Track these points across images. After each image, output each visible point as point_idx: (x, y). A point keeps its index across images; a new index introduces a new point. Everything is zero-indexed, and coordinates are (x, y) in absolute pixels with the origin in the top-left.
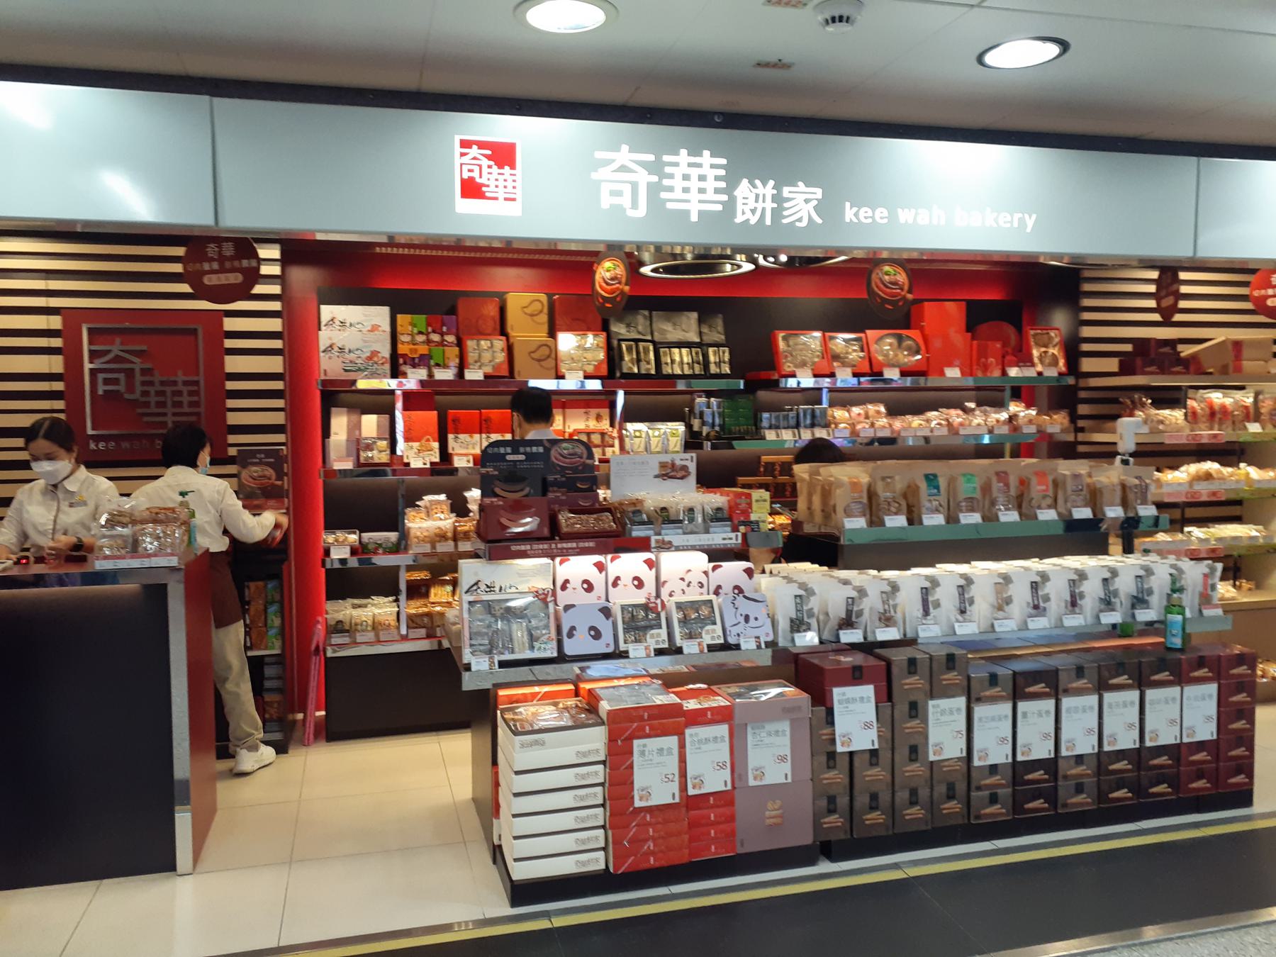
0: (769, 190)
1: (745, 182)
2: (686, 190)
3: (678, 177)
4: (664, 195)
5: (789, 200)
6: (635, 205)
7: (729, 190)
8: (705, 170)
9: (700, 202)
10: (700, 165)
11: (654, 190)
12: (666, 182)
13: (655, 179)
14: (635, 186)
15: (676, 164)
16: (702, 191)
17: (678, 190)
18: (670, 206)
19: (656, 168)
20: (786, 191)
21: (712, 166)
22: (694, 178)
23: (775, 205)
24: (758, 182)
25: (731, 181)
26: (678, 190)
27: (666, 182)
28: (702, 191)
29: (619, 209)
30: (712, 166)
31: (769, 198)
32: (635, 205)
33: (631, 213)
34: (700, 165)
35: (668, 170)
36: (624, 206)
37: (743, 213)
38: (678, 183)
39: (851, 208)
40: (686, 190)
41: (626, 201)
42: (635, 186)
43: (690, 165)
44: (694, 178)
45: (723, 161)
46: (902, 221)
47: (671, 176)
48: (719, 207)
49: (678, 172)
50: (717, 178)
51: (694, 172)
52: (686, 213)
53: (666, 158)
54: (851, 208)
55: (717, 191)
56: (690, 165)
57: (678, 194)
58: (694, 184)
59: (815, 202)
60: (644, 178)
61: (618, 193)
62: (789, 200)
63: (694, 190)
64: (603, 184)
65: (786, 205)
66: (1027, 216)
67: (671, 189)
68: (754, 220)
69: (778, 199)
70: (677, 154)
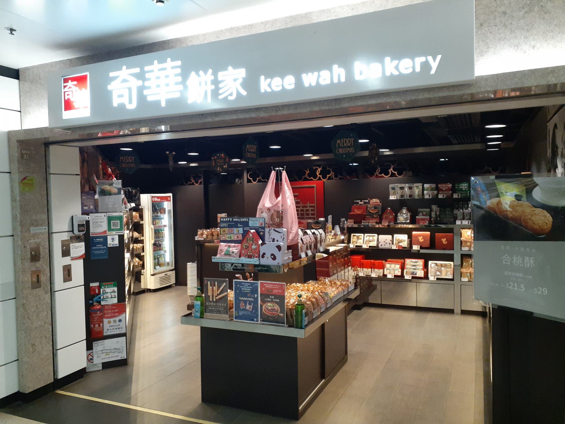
0: (209, 76)
1: (193, 74)
2: (158, 86)
5: (222, 81)
6: (130, 102)
7: (184, 82)
11: (141, 90)
13: (140, 83)
14: (130, 89)
15: (152, 71)
16: (167, 85)
18: (149, 99)
19: (141, 76)
20: (221, 75)
23: (213, 87)
24: (201, 72)
25: (185, 75)
28: (167, 85)
30: (173, 68)
31: (209, 83)
36: (125, 103)
39: (265, 80)
40: (158, 86)
45: (179, 63)
46: (306, 84)
47: (149, 79)
50: (176, 75)
54: (265, 80)
55: (177, 84)
59: (241, 80)
60: (135, 83)
61: (120, 96)
62: (222, 81)
65: (220, 86)
66: (430, 58)
69: (216, 82)
70: (152, 64)
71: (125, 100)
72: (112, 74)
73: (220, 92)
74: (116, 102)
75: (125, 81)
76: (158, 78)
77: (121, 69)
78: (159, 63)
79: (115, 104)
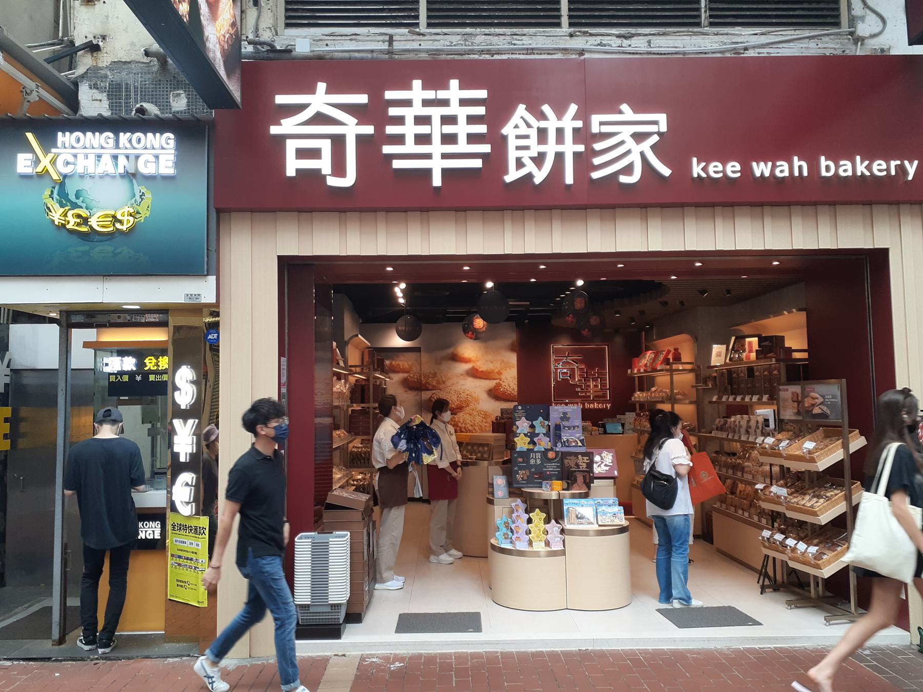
3: (410, 120)
4: (387, 149)
6: (339, 169)
8: (454, 109)
9: (445, 156)
10: (445, 103)
12: (390, 130)
15: (407, 103)
17: (410, 139)
18: (397, 164)
21: (464, 102)
22: (436, 121)
26: (410, 139)
27: (390, 130)
28: (449, 139)
29: (316, 175)
32: (339, 169)
33: (333, 182)
34: (445, 103)
35: (393, 111)
36: (324, 172)
37: (520, 164)
38: (410, 130)
41: (324, 164)
42: (338, 142)
43: (426, 103)
44: (436, 121)
45: (482, 94)
48: (477, 163)
49: (409, 113)
51: (436, 113)
52: (428, 172)
53: (389, 95)
56: (426, 103)
57: (410, 147)
58: (436, 130)
63: (437, 138)
64: (289, 142)
67: (399, 139)
68: (539, 177)
71: (324, 164)
72: (281, 99)
73: (597, 161)
74: (292, 165)
75: (320, 119)
76: (422, 120)
77: (312, 90)
78: (425, 87)
79: (291, 172)
